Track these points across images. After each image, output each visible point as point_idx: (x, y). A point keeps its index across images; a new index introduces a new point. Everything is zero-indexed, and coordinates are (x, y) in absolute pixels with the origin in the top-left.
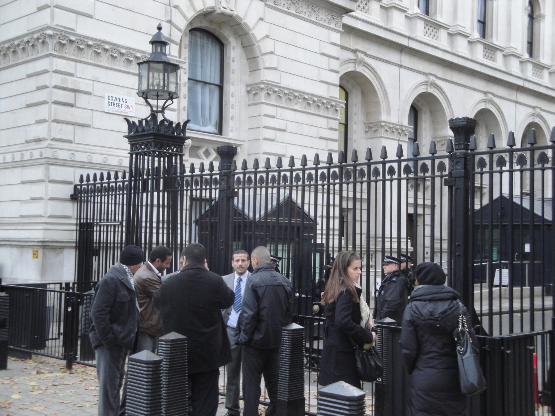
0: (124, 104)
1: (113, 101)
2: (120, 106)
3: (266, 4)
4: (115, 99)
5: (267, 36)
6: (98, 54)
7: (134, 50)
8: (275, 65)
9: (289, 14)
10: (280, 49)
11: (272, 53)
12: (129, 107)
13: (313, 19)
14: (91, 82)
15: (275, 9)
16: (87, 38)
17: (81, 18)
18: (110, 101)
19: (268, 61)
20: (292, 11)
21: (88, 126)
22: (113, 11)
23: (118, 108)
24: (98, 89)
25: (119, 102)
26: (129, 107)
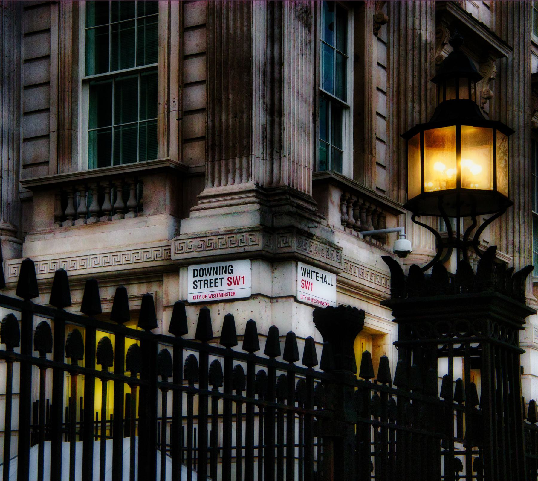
0: (226, 276)
12: (237, 281)
18: (199, 278)
23: (214, 289)
25: (215, 277)
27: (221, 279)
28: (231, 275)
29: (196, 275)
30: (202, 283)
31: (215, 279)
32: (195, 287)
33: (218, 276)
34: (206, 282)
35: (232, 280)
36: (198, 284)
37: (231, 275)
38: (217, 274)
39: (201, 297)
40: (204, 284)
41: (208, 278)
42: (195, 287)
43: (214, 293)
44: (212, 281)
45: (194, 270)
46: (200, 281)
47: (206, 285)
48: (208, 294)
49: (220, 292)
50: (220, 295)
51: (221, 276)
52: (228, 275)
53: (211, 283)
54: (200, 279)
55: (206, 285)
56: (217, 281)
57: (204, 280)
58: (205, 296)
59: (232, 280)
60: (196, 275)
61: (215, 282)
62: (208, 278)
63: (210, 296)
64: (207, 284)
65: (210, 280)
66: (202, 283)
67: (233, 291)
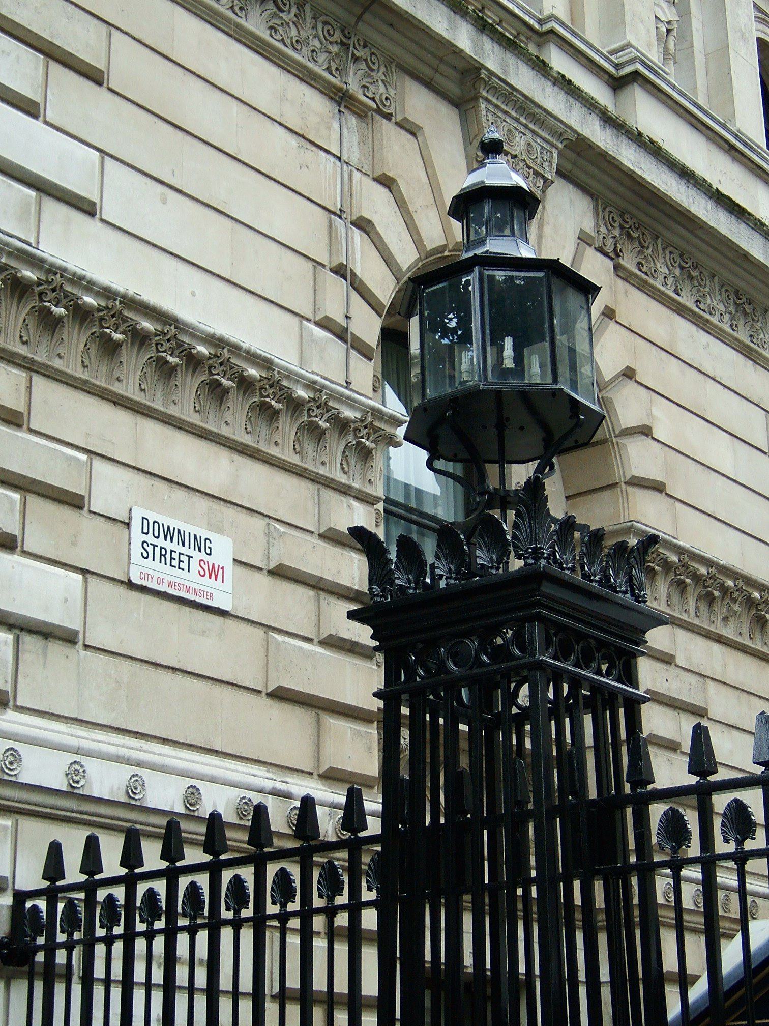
0: (197, 556)
1: (161, 542)
2: (184, 565)
3: (617, 268)
4: (168, 534)
5: (629, 374)
6: (110, 349)
7: (235, 349)
8: (655, 474)
9: (681, 310)
10: (667, 423)
11: (645, 431)
12: (214, 572)
13: (743, 335)
14: (83, 457)
15: (643, 287)
16: (78, 280)
17: (53, 209)
18: (150, 538)
19: (640, 458)
20: (687, 300)
21: (69, 638)
22: (164, 201)
24: (109, 490)
25: (179, 549)
26: (214, 572)
27: (190, 557)
28: (206, 558)
29: (145, 531)
30: (157, 550)
31: (180, 554)
32: (145, 555)
33: (185, 550)
34: (163, 552)
35: (206, 567)
36: (150, 549)
37: (206, 558)
38: (184, 545)
39: (155, 579)
40: (161, 555)
41: (168, 545)
42: (145, 555)
43: (178, 581)
44: (174, 555)
45: (143, 518)
46: (154, 546)
47: (163, 558)
48: (167, 578)
49: (188, 584)
50: (188, 590)
51: (191, 552)
52: (203, 555)
53: (171, 558)
54: (155, 541)
55: (163, 558)
56: (182, 558)
57: (161, 548)
58: (161, 581)
59: (206, 567)
60: (145, 531)
61: (180, 561)
62: (168, 545)
63: (170, 585)
64: (164, 556)
65: (172, 551)
66: (157, 550)
67: (210, 590)
